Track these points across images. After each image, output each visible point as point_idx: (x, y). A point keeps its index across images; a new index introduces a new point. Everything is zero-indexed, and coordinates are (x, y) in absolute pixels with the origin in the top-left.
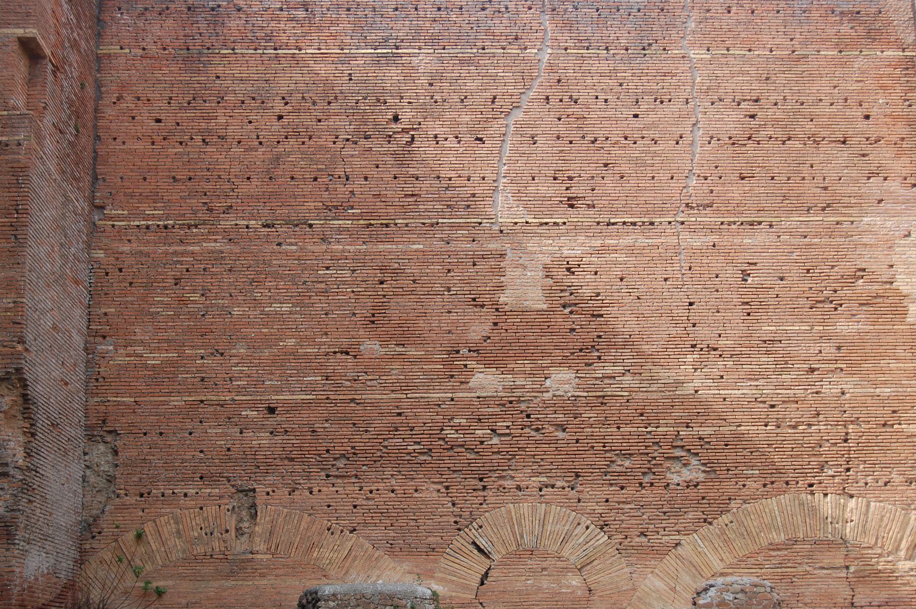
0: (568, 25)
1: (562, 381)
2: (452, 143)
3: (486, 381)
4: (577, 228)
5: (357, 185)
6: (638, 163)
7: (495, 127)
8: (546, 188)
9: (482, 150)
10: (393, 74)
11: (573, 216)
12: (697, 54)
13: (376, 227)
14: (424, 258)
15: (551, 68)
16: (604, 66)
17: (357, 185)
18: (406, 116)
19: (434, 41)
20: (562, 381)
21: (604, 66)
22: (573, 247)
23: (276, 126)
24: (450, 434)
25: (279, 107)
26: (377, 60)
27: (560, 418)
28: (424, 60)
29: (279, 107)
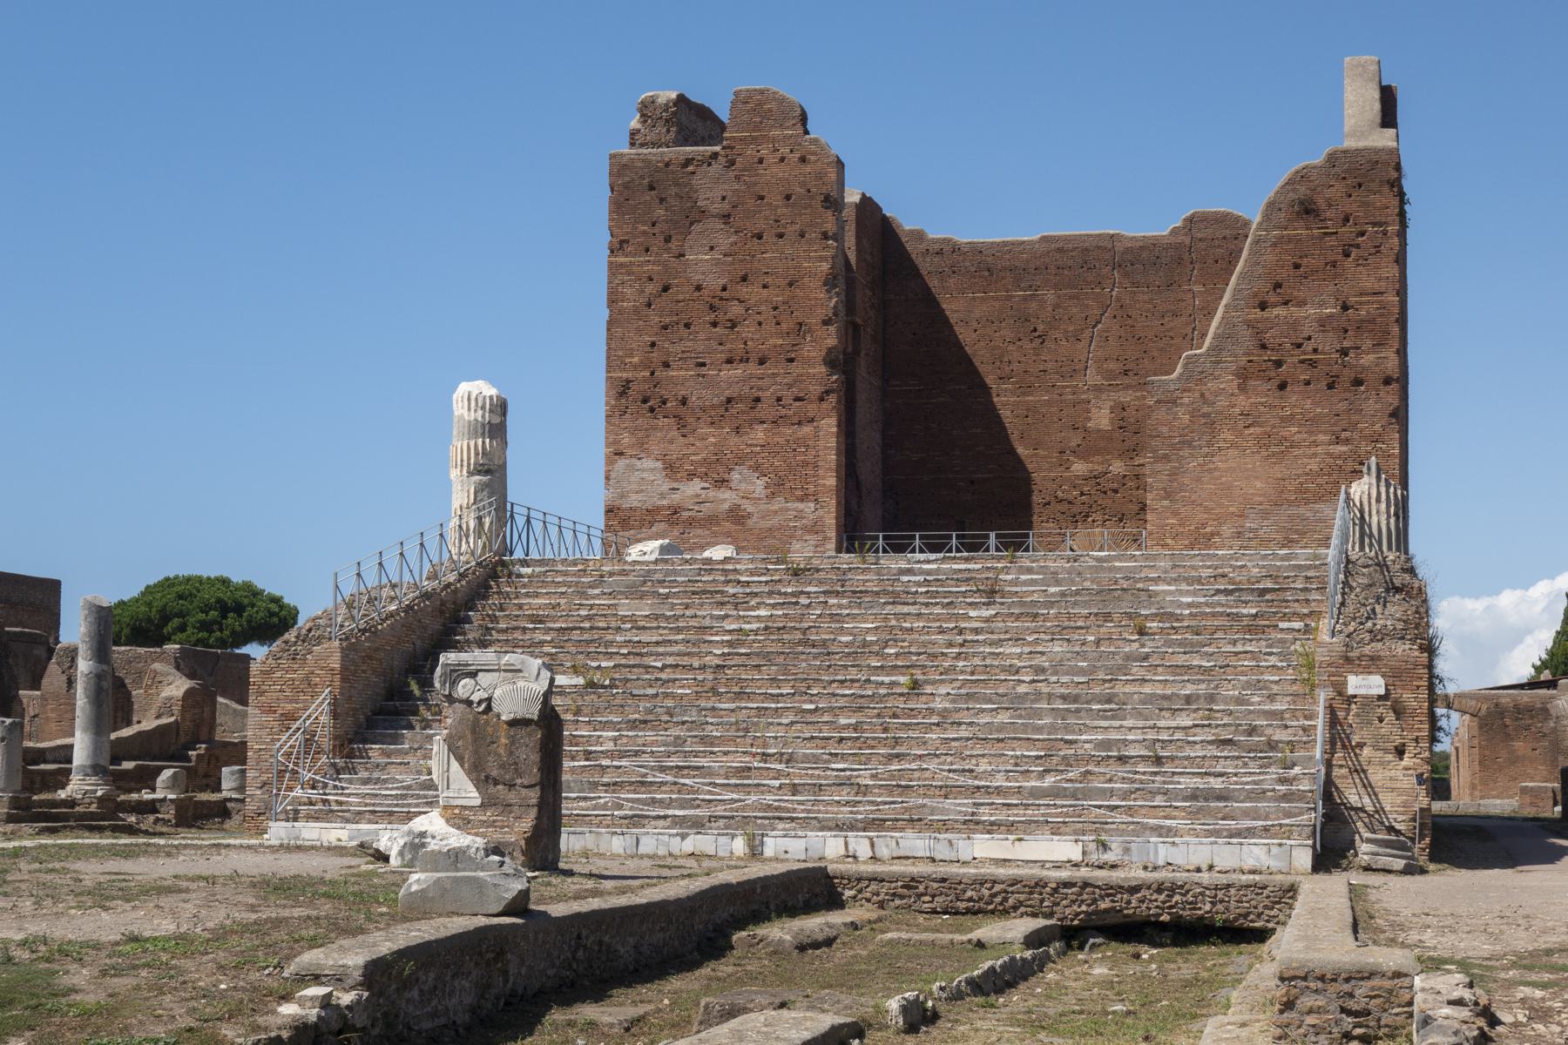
0: (1126, 275)
1: (1117, 467)
2: (1064, 342)
3: (1079, 468)
4: (1128, 387)
5: (1015, 366)
6: (1161, 350)
7: (1088, 333)
8: (1112, 365)
9: (1080, 345)
10: (1034, 304)
11: (1127, 380)
12: (1197, 288)
13: (1027, 389)
14: (1049, 403)
15: (1118, 299)
16: (1146, 297)
17: (1015, 366)
18: (1041, 327)
19: (1056, 287)
20: (1117, 467)
21: (1146, 297)
22: (1126, 397)
23: (974, 335)
24: (1060, 494)
25: (975, 325)
26: (1025, 298)
27: (1115, 485)
28: (1050, 296)
29: (975, 325)
